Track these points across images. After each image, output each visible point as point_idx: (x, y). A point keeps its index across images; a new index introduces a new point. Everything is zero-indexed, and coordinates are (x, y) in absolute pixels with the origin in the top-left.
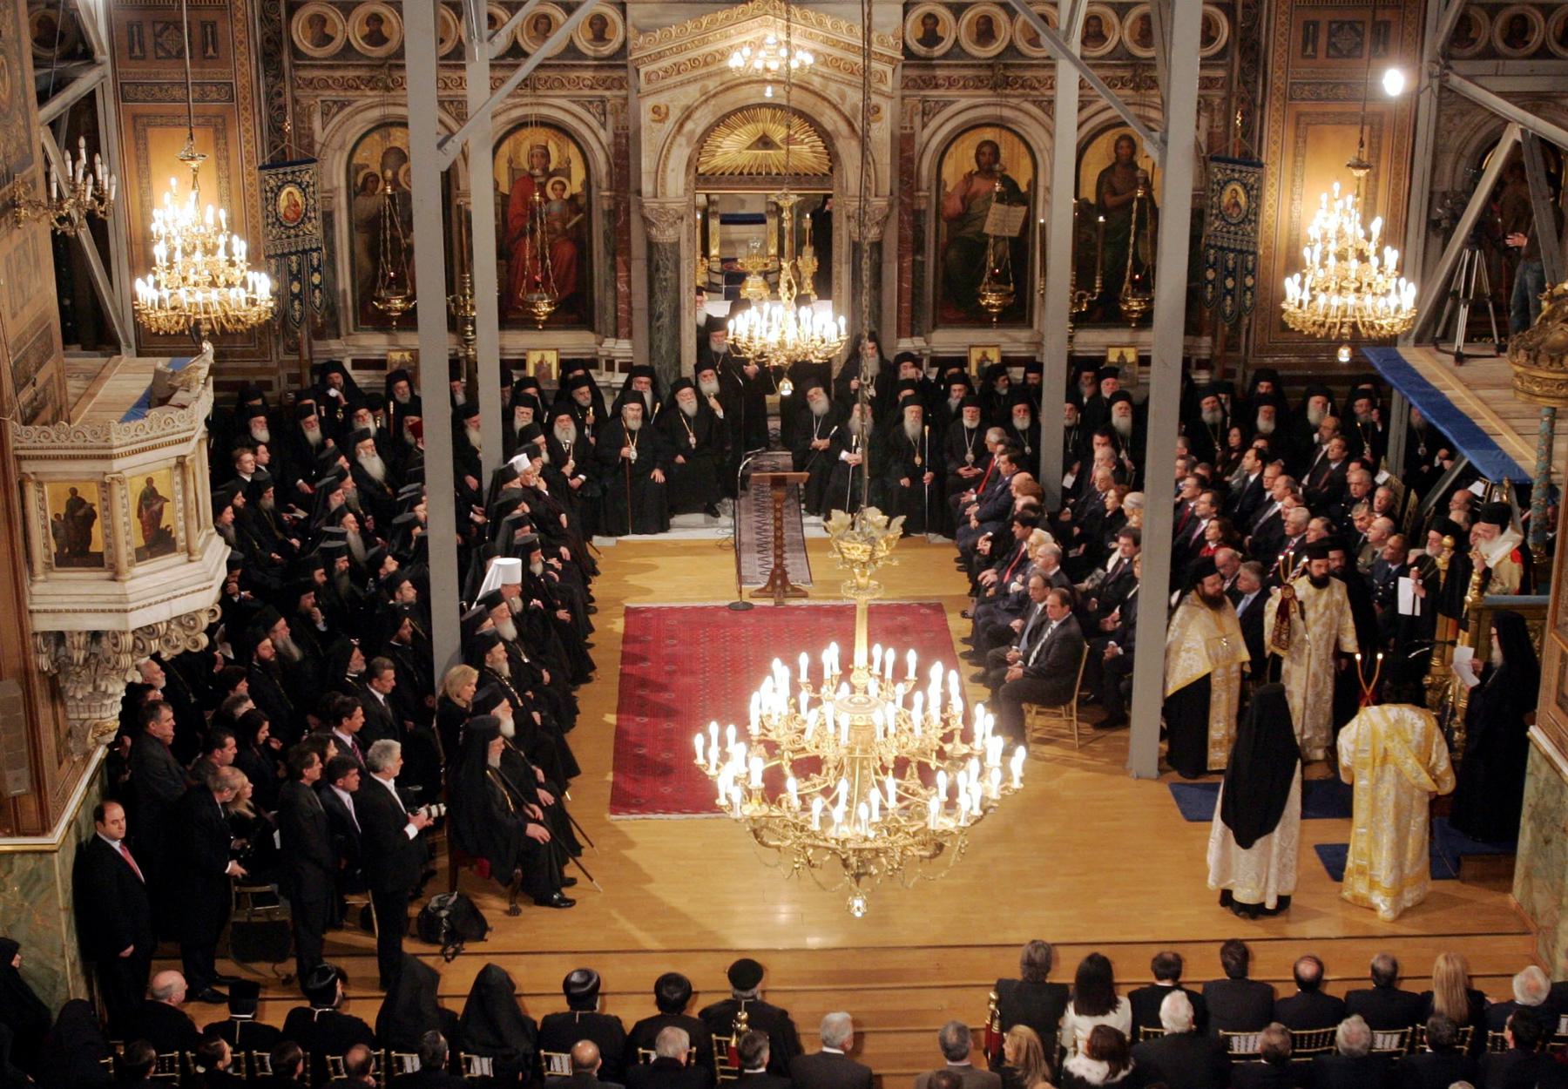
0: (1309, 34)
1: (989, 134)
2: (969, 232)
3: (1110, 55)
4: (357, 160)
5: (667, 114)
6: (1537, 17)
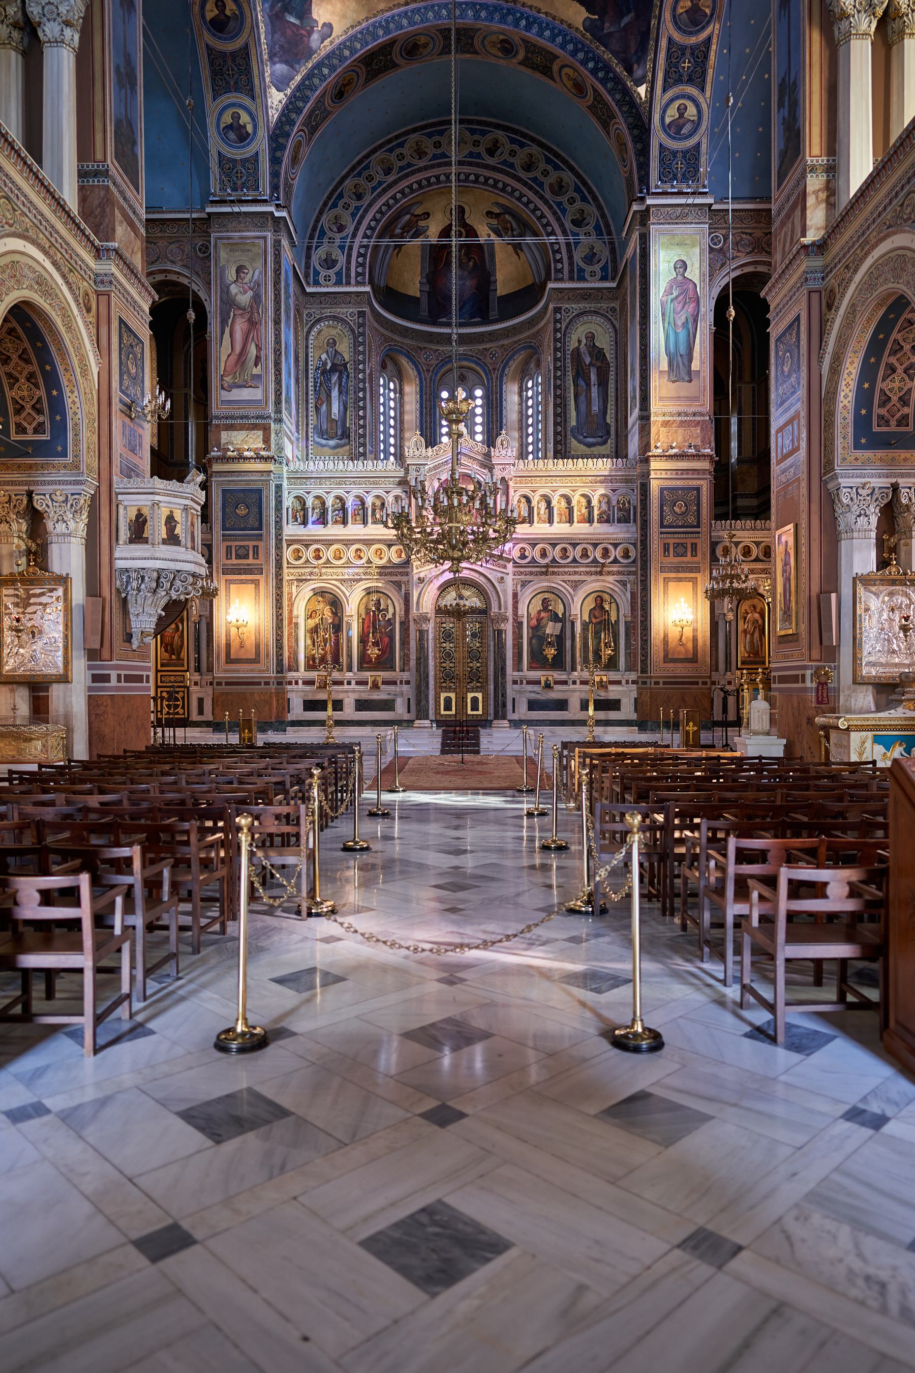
0: (666, 548)
1: (546, 595)
2: (539, 633)
3: (592, 562)
6: (754, 548)
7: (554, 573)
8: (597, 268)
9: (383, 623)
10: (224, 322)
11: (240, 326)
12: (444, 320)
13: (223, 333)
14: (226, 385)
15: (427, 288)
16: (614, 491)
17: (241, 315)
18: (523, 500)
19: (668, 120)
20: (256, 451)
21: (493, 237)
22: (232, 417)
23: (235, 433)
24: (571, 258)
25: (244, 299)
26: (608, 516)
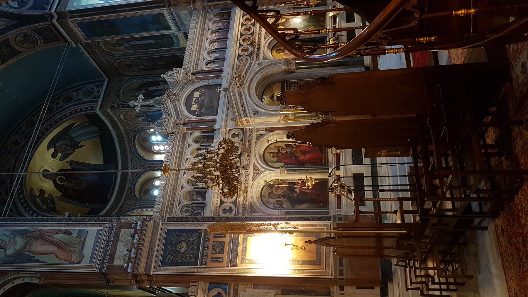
4: (271, 206)
5: (256, 111)
7: (259, 45)
8: (96, 89)
9: (289, 150)
10: (31, 260)
11: (39, 247)
12: (109, 196)
13: (38, 261)
14: (78, 260)
15: (87, 204)
16: (210, 20)
17: (30, 245)
18: (209, 66)
19: (16, 6)
20: (136, 232)
21: (68, 159)
22: (104, 255)
23: (118, 252)
24: (86, 102)
25: (20, 242)
26: (225, 22)
